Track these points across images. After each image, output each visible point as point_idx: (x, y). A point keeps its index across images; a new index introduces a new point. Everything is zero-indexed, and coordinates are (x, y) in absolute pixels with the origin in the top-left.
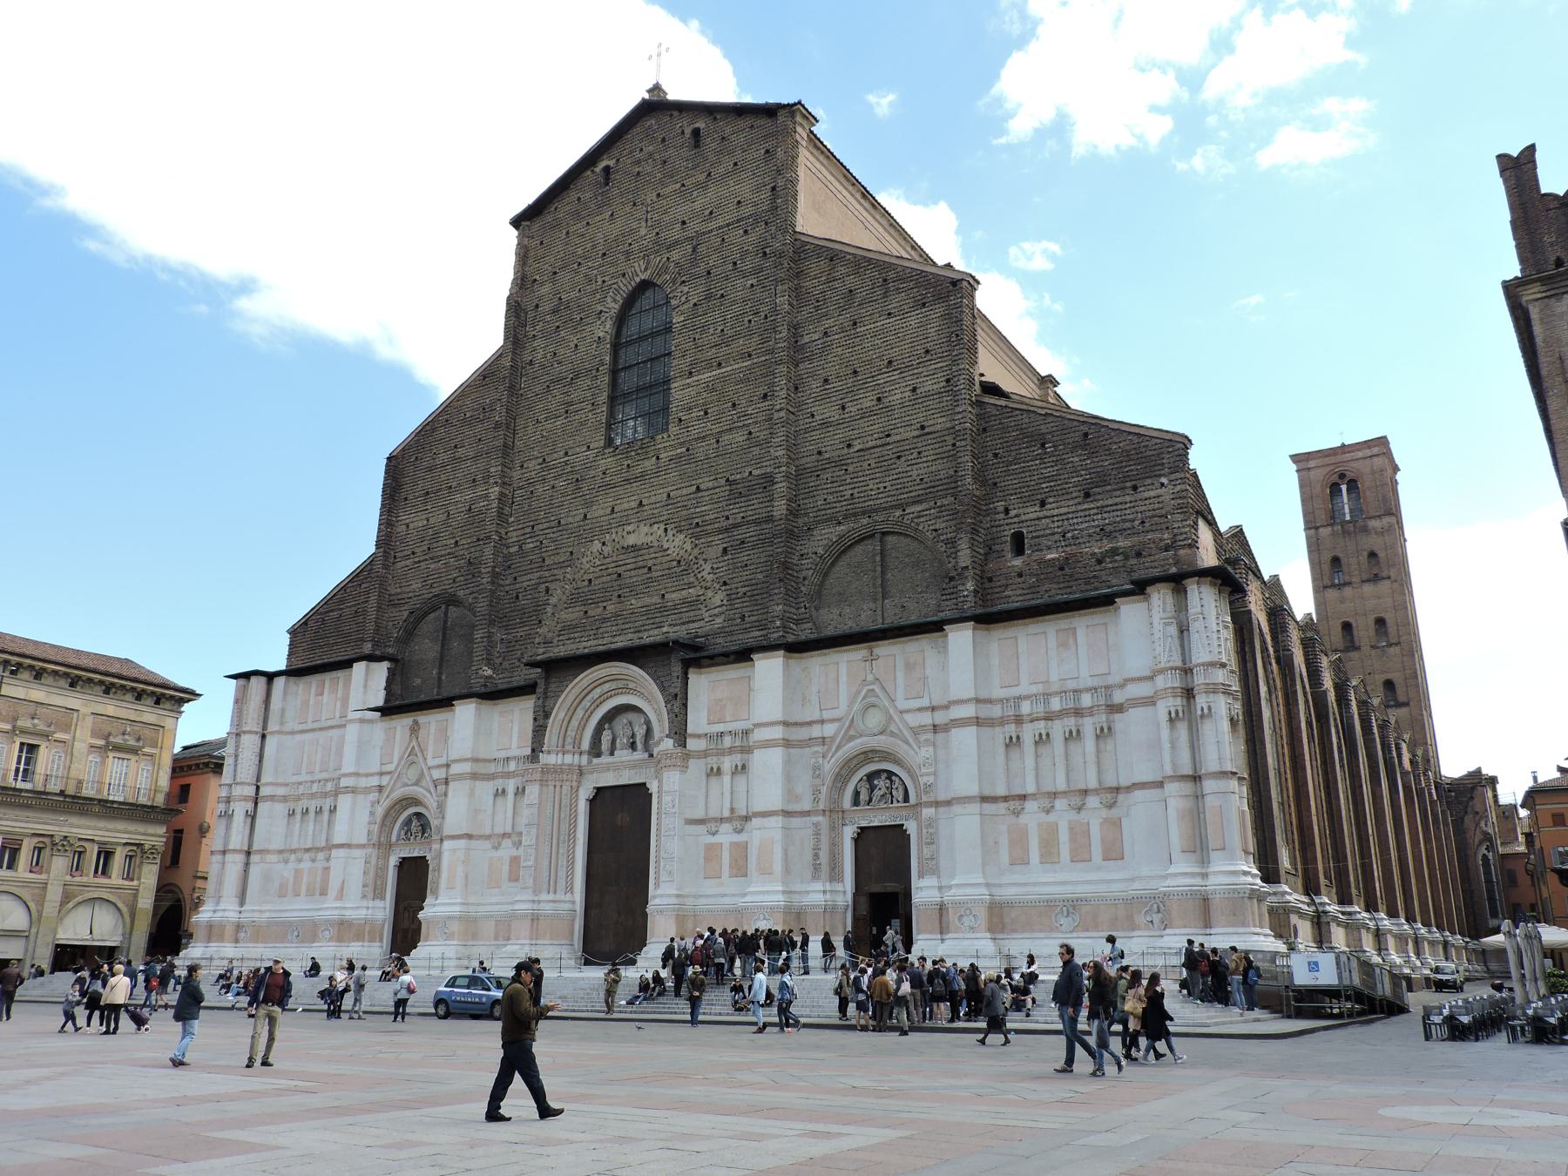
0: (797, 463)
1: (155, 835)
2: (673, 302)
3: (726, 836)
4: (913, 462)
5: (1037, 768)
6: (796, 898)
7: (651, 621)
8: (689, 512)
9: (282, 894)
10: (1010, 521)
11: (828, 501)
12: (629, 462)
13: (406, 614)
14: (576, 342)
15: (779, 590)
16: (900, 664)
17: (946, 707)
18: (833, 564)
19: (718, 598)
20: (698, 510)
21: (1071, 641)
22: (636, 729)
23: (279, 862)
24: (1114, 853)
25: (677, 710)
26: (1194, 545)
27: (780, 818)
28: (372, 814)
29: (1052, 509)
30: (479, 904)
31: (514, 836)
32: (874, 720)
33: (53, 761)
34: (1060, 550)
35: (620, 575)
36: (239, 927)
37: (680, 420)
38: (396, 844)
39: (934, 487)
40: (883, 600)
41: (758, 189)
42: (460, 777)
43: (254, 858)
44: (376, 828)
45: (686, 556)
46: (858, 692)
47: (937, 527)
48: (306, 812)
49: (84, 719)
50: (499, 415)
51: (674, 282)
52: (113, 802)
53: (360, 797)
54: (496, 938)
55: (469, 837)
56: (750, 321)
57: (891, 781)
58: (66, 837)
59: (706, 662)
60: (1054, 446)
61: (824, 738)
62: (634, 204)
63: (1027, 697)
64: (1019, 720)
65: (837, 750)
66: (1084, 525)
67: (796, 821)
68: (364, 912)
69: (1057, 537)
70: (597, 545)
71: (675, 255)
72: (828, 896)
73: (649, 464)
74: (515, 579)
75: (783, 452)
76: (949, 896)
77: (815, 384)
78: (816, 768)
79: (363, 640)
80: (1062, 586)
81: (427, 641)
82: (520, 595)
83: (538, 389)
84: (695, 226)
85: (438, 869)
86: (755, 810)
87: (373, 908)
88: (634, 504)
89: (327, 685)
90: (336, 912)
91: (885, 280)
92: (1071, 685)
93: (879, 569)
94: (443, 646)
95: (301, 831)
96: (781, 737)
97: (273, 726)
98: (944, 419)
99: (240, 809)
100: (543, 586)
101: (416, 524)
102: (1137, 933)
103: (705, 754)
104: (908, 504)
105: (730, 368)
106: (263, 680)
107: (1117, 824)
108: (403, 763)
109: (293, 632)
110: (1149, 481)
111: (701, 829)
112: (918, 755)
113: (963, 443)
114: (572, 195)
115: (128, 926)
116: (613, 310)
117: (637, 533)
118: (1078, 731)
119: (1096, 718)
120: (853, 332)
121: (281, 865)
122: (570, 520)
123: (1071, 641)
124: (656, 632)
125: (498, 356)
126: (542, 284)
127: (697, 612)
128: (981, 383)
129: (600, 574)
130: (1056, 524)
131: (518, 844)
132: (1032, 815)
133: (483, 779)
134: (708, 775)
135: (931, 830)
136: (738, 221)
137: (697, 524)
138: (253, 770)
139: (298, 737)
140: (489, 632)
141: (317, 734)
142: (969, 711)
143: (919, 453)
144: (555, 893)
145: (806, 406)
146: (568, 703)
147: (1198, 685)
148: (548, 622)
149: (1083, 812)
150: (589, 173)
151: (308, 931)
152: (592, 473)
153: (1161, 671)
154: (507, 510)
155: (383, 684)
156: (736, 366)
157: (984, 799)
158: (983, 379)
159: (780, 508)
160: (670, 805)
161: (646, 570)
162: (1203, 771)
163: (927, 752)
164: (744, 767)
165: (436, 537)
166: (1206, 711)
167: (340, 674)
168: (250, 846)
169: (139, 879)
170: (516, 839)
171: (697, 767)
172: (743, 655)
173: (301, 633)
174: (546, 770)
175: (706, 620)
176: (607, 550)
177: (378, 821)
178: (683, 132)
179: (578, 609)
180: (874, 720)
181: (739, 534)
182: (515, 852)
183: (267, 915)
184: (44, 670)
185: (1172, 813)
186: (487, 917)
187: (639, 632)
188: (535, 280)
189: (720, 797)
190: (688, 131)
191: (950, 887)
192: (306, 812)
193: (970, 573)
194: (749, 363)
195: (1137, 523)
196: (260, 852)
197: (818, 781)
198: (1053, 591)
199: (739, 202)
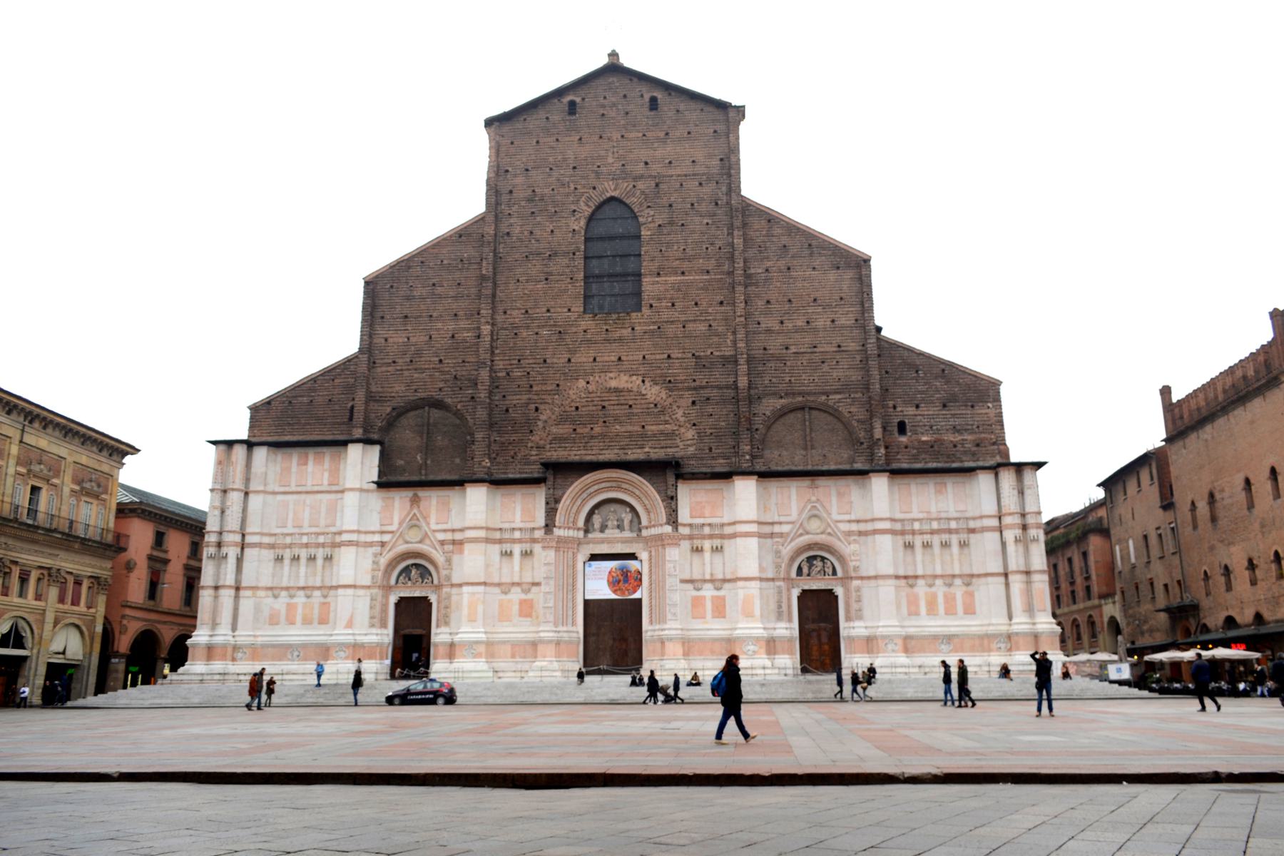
2: (641, 219)
3: (708, 592)
5: (923, 561)
11: (774, 380)
13: (389, 409)
14: (551, 228)
15: (745, 436)
16: (834, 492)
17: (866, 521)
19: (690, 433)
20: (670, 371)
21: (944, 490)
23: (268, 597)
24: (970, 610)
25: (674, 507)
27: (758, 582)
29: (924, 410)
30: (492, 633)
35: (604, 407)
36: (236, 648)
37: (651, 306)
41: (710, 156)
43: (242, 593)
44: (380, 574)
46: (805, 507)
47: (851, 410)
48: (296, 559)
50: (486, 269)
51: (641, 204)
53: (361, 549)
55: (485, 584)
56: (707, 248)
57: (824, 563)
58: (59, 570)
61: (782, 533)
62: (601, 137)
64: (913, 533)
65: (790, 542)
66: (944, 423)
67: (765, 584)
70: (582, 383)
71: (641, 185)
73: (626, 332)
74: (504, 396)
75: (744, 345)
77: (760, 303)
78: (778, 553)
81: (407, 432)
82: (510, 410)
84: (656, 169)
87: (381, 634)
89: (311, 457)
91: (810, 245)
92: (943, 515)
93: (808, 430)
95: (290, 573)
97: (253, 487)
99: (232, 553)
102: (992, 654)
103: (691, 537)
105: (692, 278)
106: (245, 446)
107: (971, 595)
108: (404, 525)
109: (255, 409)
110: (981, 404)
111: (690, 586)
112: (847, 549)
113: (874, 363)
114: (541, 113)
115: (88, 647)
116: (587, 214)
117: (618, 380)
119: (958, 536)
121: (270, 600)
122: (555, 360)
123: (944, 490)
124: (639, 451)
125: (480, 220)
126: (515, 176)
127: (673, 442)
129: (586, 404)
131: (527, 591)
132: (921, 588)
136: (694, 175)
137: (670, 381)
138: (240, 520)
139: (280, 497)
141: (303, 497)
142: (886, 525)
146: (574, 494)
150: (556, 101)
152: (574, 330)
153: (1010, 514)
156: (697, 277)
157: (897, 577)
159: (743, 382)
160: (673, 570)
162: (1032, 569)
163: (853, 547)
164: (722, 547)
165: (419, 353)
167: (328, 452)
169: (96, 607)
170: (525, 587)
171: (686, 545)
173: (260, 412)
174: (561, 541)
175: (682, 447)
176: (591, 388)
177: (382, 567)
178: (642, 96)
179: (567, 426)
180: (814, 525)
182: (523, 596)
183: (260, 639)
186: (504, 642)
188: (507, 171)
190: (647, 97)
193: (881, 443)
194: (708, 277)
195: (974, 427)
197: (779, 560)
198: (928, 460)
199: (693, 162)
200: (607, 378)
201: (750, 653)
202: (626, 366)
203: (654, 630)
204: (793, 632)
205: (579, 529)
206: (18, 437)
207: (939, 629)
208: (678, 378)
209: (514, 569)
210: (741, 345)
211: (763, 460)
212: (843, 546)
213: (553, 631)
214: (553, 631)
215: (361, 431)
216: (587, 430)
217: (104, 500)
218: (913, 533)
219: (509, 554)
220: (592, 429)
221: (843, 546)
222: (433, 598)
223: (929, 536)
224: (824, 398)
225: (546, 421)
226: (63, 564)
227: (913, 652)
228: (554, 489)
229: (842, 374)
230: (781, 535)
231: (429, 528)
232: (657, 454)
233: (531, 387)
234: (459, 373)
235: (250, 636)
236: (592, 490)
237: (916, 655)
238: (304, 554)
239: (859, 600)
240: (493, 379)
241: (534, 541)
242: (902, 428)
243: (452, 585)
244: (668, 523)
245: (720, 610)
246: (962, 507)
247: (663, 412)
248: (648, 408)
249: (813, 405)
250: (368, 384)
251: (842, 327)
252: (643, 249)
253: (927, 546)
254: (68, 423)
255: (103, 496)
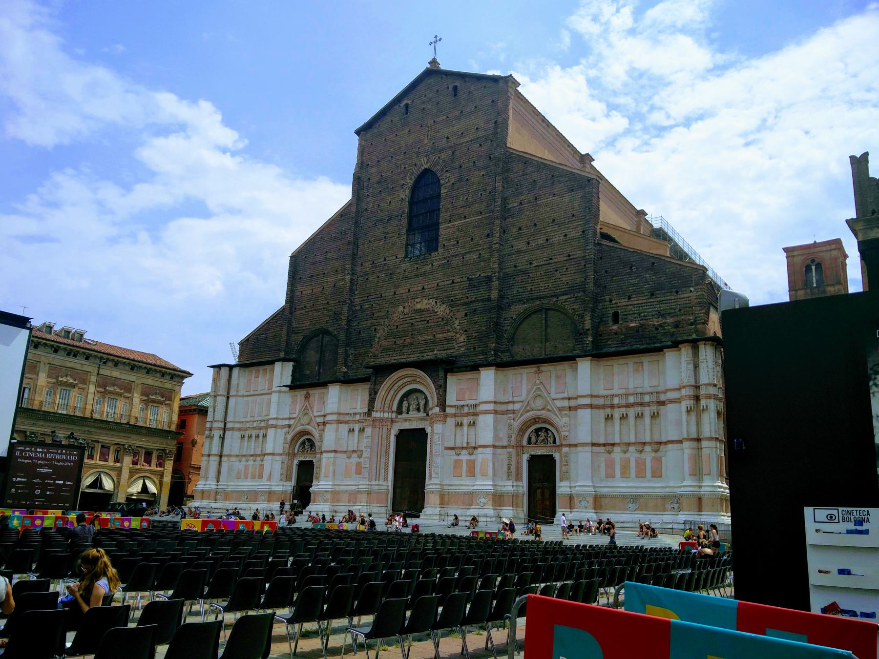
0: (503, 271)
1: (171, 446)
2: (442, 182)
3: (464, 456)
4: (564, 273)
5: (620, 430)
6: (499, 488)
7: (428, 348)
8: (448, 293)
9: (238, 478)
10: (612, 306)
12: (418, 266)
15: (493, 336)
17: (576, 398)
18: (521, 323)
19: (462, 338)
20: (453, 293)
22: (420, 401)
25: (441, 393)
26: (706, 322)
28: (285, 439)
31: (359, 453)
32: (539, 403)
33: (123, 408)
34: (637, 322)
35: (412, 324)
37: (444, 246)
38: (297, 454)
39: (573, 287)
40: (546, 342)
42: (331, 422)
43: (224, 459)
44: (287, 446)
45: (446, 316)
47: (574, 307)
48: (250, 437)
49: (137, 386)
50: (350, 237)
51: (442, 170)
52: (152, 428)
53: (279, 430)
55: (336, 451)
56: (481, 194)
58: (130, 445)
59: (456, 370)
60: (636, 268)
61: (514, 410)
63: (617, 396)
64: (612, 406)
67: (499, 451)
68: (281, 487)
69: (636, 315)
70: (401, 308)
71: (443, 156)
72: (515, 488)
74: (359, 323)
75: (497, 266)
76: (574, 491)
77: (514, 230)
79: (279, 350)
80: (637, 340)
83: (370, 224)
85: (319, 467)
86: (479, 444)
87: (286, 485)
88: (420, 288)
89: (261, 372)
90: (268, 487)
92: (639, 390)
93: (544, 327)
94: (321, 355)
96: (493, 409)
97: (232, 392)
98: (578, 252)
99: (217, 434)
100: (374, 327)
101: (306, 292)
103: (455, 415)
104: (560, 295)
105: (470, 219)
107: (659, 460)
109: (242, 344)
110: (684, 289)
111: (453, 452)
112: (561, 421)
113: (589, 265)
116: (410, 184)
118: (642, 414)
120: (535, 203)
121: (238, 463)
122: (387, 294)
124: (431, 354)
125: (349, 205)
127: (452, 345)
128: (600, 232)
130: (636, 309)
131: (360, 456)
132: (617, 454)
133: (343, 423)
134: (456, 426)
135: (567, 459)
137: (452, 300)
138: (223, 414)
139: (246, 399)
140: (345, 349)
141: (256, 397)
143: (567, 269)
144: (379, 480)
145: (509, 242)
147: (702, 395)
148: (376, 346)
149: (643, 454)
151: (253, 495)
152: (398, 271)
154: (354, 287)
155: (290, 373)
156: (474, 218)
157: (593, 445)
158: (602, 231)
159: (494, 295)
161: (426, 322)
162: (702, 437)
163: (565, 420)
166: (705, 407)
167: (268, 367)
168: (222, 451)
171: (451, 421)
172: (475, 368)
176: (406, 311)
177: (288, 442)
180: (539, 403)
181: (473, 306)
182: (358, 460)
183: (231, 487)
184: (119, 361)
185: (686, 456)
186: (345, 492)
187: (422, 353)
189: (462, 437)
191: (575, 487)
192: (250, 437)
195: (677, 310)
196: (227, 456)
200: (415, 303)
201: (481, 504)
202: (427, 292)
204: (521, 489)
205: (392, 413)
206: (96, 372)
207: (629, 490)
208: (458, 297)
209: (352, 442)
211: (508, 354)
212: (558, 420)
213: (366, 484)
214: (366, 484)
215: (283, 353)
216: (402, 341)
217: (169, 405)
218: (612, 406)
219: (352, 431)
221: (558, 420)
222: (314, 461)
223: (624, 408)
224: (555, 299)
225: (379, 338)
226: (134, 442)
227: (606, 509)
228: (375, 384)
229: (570, 278)
231: (313, 415)
232: (442, 354)
233: (373, 315)
234: (336, 310)
235: (224, 485)
237: (607, 511)
238: (254, 433)
242: (616, 318)
243: (321, 453)
245: (471, 472)
246: (655, 383)
247: (446, 324)
248: (438, 322)
249: (547, 306)
250: (290, 323)
251: (572, 239)
252: (441, 204)
254: (131, 362)
255: (167, 402)
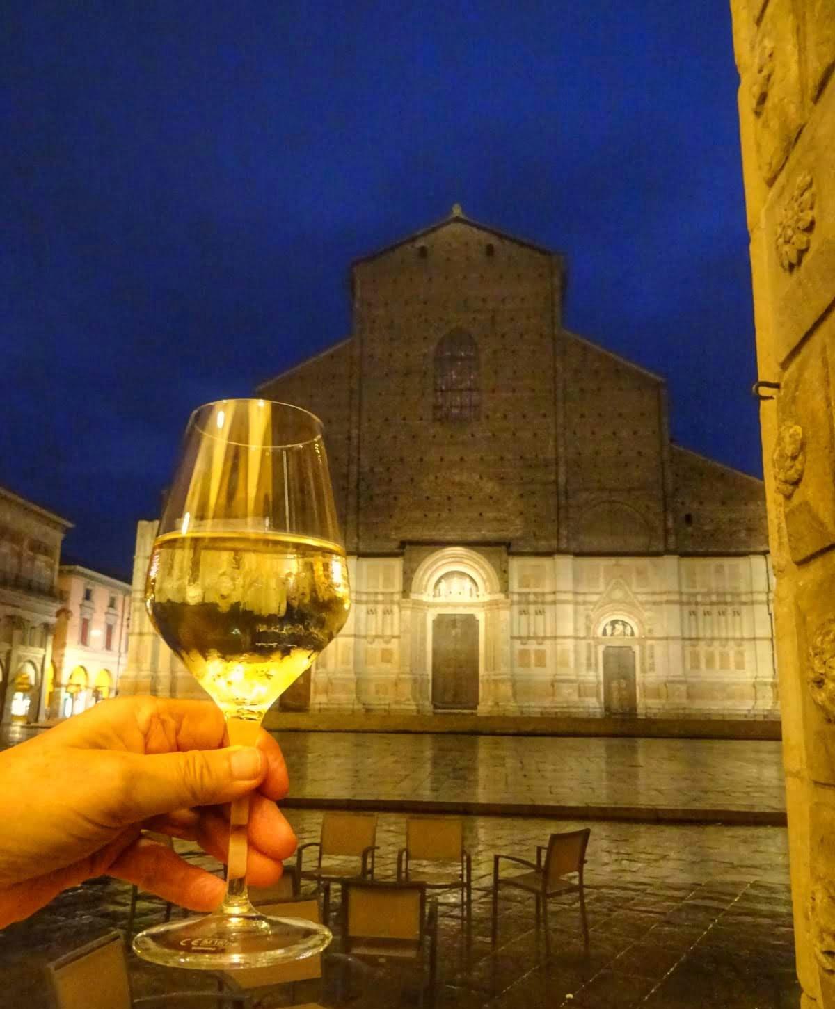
3: (532, 646)
19: (518, 521)
37: (488, 417)
54: (377, 692)
55: (355, 636)
78: (588, 617)
88: (457, 458)
92: (721, 590)
103: (519, 603)
107: (741, 654)
111: (519, 641)
119: (732, 607)
150: (409, 246)
157: (683, 639)
159: (562, 479)
163: (647, 614)
170: (386, 639)
171: (516, 608)
182: (384, 646)
203: (489, 675)
210: (561, 450)
216: (436, 515)
218: (697, 603)
220: (439, 515)
230: (590, 603)
233: (391, 480)
236: (440, 563)
239: (652, 657)
240: (359, 473)
241: (392, 602)
242: (688, 519)
244: (501, 591)
247: (497, 502)
253: (707, 613)
